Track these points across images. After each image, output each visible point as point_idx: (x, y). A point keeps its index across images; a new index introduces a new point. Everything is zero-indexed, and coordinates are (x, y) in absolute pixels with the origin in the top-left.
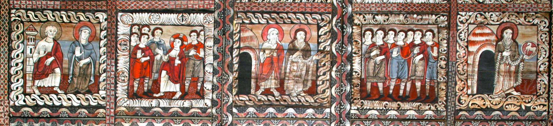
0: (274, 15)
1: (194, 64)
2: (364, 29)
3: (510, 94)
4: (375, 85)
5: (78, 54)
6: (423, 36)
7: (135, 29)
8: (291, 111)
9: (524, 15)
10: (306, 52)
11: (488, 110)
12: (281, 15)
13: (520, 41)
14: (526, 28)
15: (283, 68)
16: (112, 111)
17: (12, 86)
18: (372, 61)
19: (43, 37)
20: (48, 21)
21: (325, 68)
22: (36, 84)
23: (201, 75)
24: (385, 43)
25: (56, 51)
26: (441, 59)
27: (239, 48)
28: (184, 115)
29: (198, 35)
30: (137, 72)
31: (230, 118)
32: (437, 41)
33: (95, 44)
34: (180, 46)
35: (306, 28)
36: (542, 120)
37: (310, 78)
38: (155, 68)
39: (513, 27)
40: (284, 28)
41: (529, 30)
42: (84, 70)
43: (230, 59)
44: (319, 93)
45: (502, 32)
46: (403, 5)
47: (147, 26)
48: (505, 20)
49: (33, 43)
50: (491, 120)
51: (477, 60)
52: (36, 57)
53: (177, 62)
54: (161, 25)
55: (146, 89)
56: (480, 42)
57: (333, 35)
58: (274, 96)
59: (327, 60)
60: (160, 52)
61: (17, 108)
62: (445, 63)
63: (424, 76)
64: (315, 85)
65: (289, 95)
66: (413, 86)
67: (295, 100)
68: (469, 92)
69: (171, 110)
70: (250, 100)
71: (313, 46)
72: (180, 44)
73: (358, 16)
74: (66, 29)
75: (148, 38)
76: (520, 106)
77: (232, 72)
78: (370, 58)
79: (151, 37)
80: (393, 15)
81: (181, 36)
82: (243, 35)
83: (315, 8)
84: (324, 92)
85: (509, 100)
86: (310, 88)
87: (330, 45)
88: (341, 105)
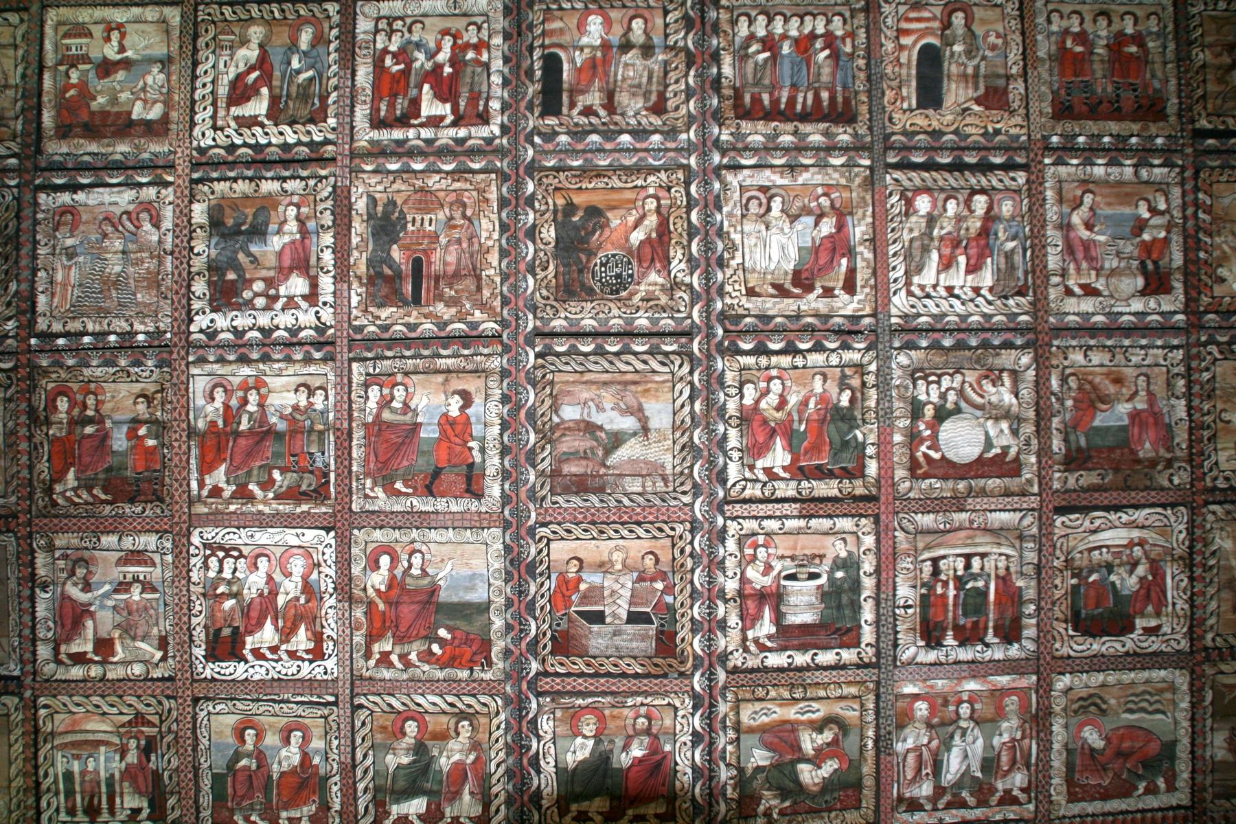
1: (473, 72)
2: (735, 14)
3: (968, 109)
5: (295, 64)
6: (829, 22)
7: (383, 25)
10: (647, 50)
11: (936, 134)
13: (979, 30)
16: (347, 147)
17: (197, 117)
18: (751, 61)
19: (244, 42)
20: (252, 18)
23: (484, 88)
24: (770, 34)
25: (263, 63)
27: (543, 46)
28: (459, 149)
29: (479, 28)
30: (385, 88)
33: (321, 49)
35: (646, 14)
36: (1020, 148)
37: (654, 88)
41: (990, 13)
42: (304, 88)
43: (529, 62)
47: (402, 19)
49: (228, 52)
50: (941, 149)
53: (448, 70)
55: (398, 112)
57: (688, 22)
58: (598, 116)
59: (679, 61)
60: (421, 56)
61: (202, 151)
62: (864, 61)
63: (833, 83)
64: (662, 98)
65: (623, 114)
66: (817, 97)
67: (633, 122)
68: (905, 106)
70: (561, 124)
71: (657, 39)
72: (451, 43)
74: (279, 29)
76: (985, 127)
77: (532, 82)
78: (747, 56)
79: (407, 35)
81: (453, 31)
84: (677, 108)
86: (655, 104)
87: (685, 38)
88: (704, 127)
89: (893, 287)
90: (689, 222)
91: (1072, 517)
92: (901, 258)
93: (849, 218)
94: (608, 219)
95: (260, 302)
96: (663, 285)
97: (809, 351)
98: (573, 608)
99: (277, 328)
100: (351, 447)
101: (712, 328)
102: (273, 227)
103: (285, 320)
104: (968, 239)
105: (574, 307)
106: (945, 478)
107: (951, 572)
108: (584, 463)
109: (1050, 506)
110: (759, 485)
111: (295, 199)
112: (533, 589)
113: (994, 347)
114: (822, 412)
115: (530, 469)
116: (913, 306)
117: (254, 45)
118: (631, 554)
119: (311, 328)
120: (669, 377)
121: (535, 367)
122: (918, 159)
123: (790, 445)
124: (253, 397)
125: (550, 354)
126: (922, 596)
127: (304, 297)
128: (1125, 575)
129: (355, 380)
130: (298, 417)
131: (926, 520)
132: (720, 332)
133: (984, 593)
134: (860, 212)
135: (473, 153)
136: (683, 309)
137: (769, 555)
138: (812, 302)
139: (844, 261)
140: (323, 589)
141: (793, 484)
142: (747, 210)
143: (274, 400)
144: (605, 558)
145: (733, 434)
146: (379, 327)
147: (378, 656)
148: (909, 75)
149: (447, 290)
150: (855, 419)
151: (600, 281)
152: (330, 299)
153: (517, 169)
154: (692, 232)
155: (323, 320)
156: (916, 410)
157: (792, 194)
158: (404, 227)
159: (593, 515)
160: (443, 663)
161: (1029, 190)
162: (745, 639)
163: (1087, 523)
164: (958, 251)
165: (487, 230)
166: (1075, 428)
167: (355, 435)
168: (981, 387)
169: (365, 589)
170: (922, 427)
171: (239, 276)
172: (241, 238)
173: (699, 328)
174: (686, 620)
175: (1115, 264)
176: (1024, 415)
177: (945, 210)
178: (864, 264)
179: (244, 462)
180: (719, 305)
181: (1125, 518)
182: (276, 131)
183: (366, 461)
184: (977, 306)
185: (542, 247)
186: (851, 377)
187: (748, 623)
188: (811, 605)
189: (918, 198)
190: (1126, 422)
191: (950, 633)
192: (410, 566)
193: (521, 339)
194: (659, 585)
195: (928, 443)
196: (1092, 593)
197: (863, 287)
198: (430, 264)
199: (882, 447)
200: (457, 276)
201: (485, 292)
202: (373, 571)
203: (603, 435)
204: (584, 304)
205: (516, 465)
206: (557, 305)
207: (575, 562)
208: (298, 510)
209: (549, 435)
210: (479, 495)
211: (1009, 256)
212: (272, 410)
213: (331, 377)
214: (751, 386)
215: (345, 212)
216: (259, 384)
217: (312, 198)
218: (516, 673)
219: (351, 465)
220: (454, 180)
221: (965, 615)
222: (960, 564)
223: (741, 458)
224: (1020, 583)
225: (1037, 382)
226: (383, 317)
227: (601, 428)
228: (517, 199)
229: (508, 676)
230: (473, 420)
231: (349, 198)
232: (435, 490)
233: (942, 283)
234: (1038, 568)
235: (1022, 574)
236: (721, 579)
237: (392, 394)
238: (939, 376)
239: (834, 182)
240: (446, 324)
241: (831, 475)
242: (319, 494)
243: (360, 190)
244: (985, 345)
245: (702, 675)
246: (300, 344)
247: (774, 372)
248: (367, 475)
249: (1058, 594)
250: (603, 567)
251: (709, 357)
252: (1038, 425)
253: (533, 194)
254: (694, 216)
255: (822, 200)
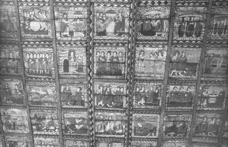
6: (45, 55)
13: (77, 56)
39: (74, 51)
45: (70, 53)
51: (63, 62)
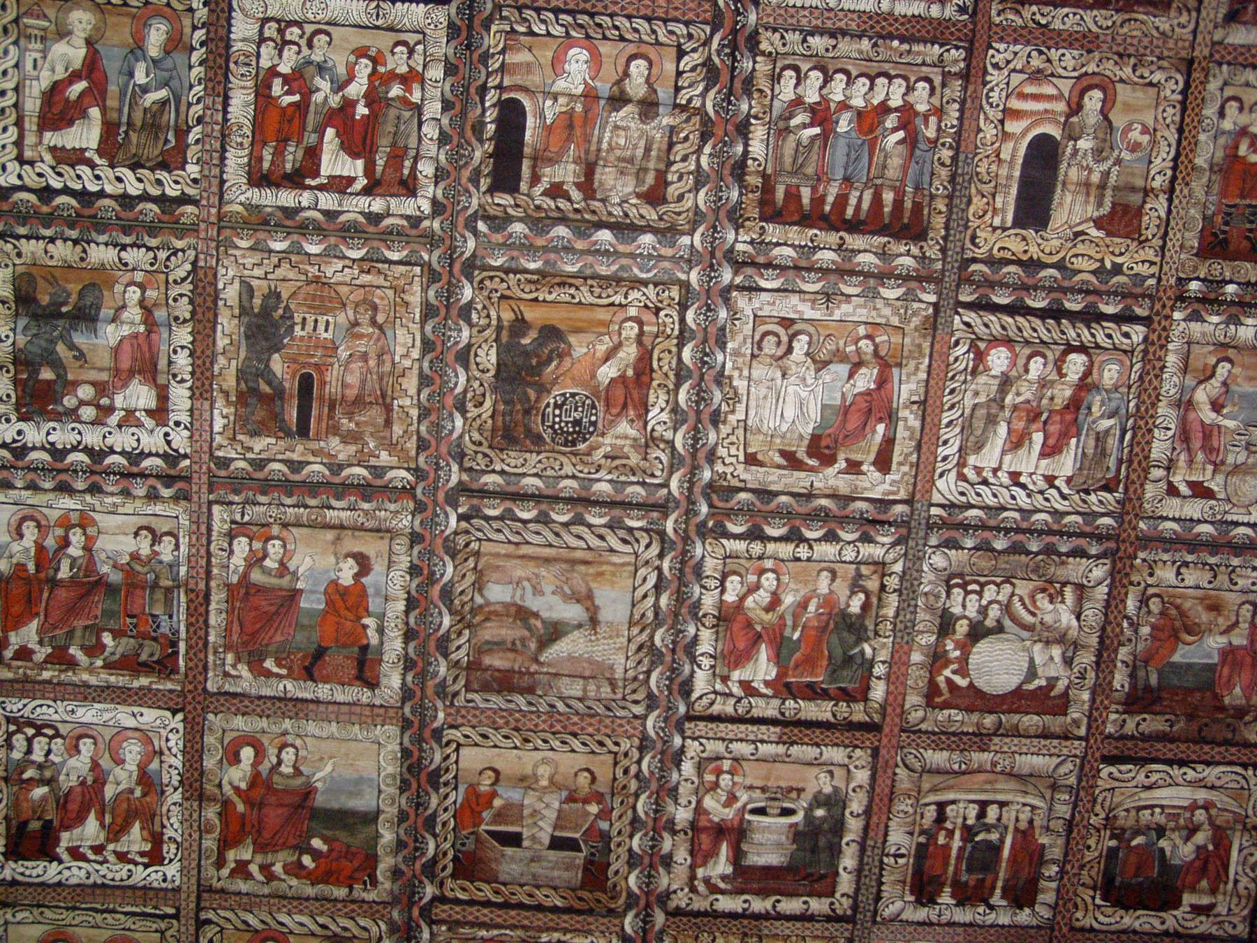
0: (583, 19)
2: (779, 65)
3: (1083, 233)
4: (793, 190)
5: (140, 77)
6: (910, 89)
7: (271, 30)
8: (605, 235)
9: (1132, 61)
10: (648, 107)
11: (1032, 265)
12: (597, 20)
13: (1118, 119)
14: (1134, 91)
15: (595, 139)
16: (214, 211)
18: (792, 137)
19: (63, 33)
21: (686, 145)
22: (45, 141)
23: (413, 142)
24: (825, 100)
25: (92, 68)
26: (943, 145)
27: (500, 87)
28: (371, 229)
29: (411, 52)
31: (471, 244)
32: (937, 104)
33: (179, 58)
34: (370, 76)
36: (1143, 296)
38: (311, 118)
39: (1107, 86)
40: (602, 50)
41: (1140, 94)
42: (154, 116)
43: (479, 111)
44: (670, 199)
46: (870, 18)
48: (1091, 68)
49: (39, 46)
50: (1035, 288)
51: (1022, 152)
52: (45, 82)
53: (362, 110)
54: (328, 23)
55: (289, 166)
56: (1033, 113)
57: (711, 74)
58: (569, 200)
59: (691, 129)
60: (324, 85)
62: (951, 153)
64: (662, 181)
65: (603, 201)
66: (877, 200)
67: (617, 211)
68: (997, 221)
69: (343, 218)
70: (517, 206)
71: (664, 94)
72: (369, 70)
73: (769, 34)
75: (299, 53)
76: (1102, 261)
77: (481, 141)
78: (787, 130)
80: (847, 39)
81: (372, 52)
82: (511, 58)
83: (676, 9)
84: (681, 198)
85: (1080, 246)
86: (652, 189)
87: (703, 95)
88: (715, 231)
89: (940, 467)
90: (680, 359)
91: (1124, 768)
92: (958, 430)
93: (895, 371)
94: (570, 346)
95: (88, 413)
96: (635, 440)
97: (818, 540)
98: (483, 827)
99: (112, 451)
100: (207, 612)
101: (694, 503)
102: (106, 312)
103: (123, 440)
104: (1051, 412)
105: (512, 460)
106: (970, 710)
107: (960, 821)
108: (511, 655)
109: (1098, 755)
110: (732, 701)
111: (139, 276)
112: (434, 801)
113: (1060, 554)
114: (824, 618)
115: (441, 659)
116: (962, 494)
117: (79, 39)
118: (562, 769)
119: (157, 455)
120: (632, 559)
121: (456, 533)
122: (1002, 299)
123: (778, 656)
124: (76, 537)
125: (477, 517)
126: (919, 845)
127: (149, 412)
128: (1178, 841)
129: (215, 528)
130: (138, 568)
131: (937, 758)
132: (704, 509)
133: (996, 849)
134: (912, 364)
135: (390, 236)
136: (658, 473)
137: (734, 784)
138: (831, 478)
139: (881, 428)
140: (165, 781)
141: (776, 702)
142: (760, 348)
143: (105, 545)
144: (528, 770)
145: (706, 635)
146: (251, 462)
147: (233, 865)
148: (1009, 177)
149: (344, 421)
150: (866, 630)
151: (552, 427)
152: (185, 418)
153: (451, 265)
154: (681, 374)
155: (174, 446)
156: (946, 624)
157: (824, 332)
158: (291, 328)
159: (517, 721)
160: (314, 878)
161: (1145, 352)
162: (693, 877)
163: (1141, 777)
164: (1034, 427)
165: (404, 345)
166: (1146, 662)
167: (214, 598)
168: (1034, 602)
169: (220, 786)
170: (950, 646)
171: (58, 376)
172: (61, 322)
173: (677, 503)
174: (622, 851)
175: (1241, 458)
176: (1084, 640)
177: (1027, 371)
178: (907, 434)
179: (63, 621)
180: (707, 475)
181: (1191, 774)
182: (112, 176)
183: (228, 629)
184: (1047, 500)
185: (477, 373)
186: (868, 577)
187: (699, 861)
188: (779, 845)
189: (993, 352)
190: (1216, 660)
191: (948, 889)
192: (280, 762)
193: (441, 496)
194: (593, 809)
195: (954, 666)
196: (1133, 859)
197: (900, 464)
198: (323, 383)
199: (895, 668)
200: (359, 402)
201: (395, 428)
202: (231, 764)
203: (539, 624)
204: (528, 455)
205: (423, 653)
206: (492, 454)
207: (490, 773)
208: (136, 684)
209: (465, 621)
210: (373, 685)
211: (1100, 438)
212: (103, 556)
213: (184, 521)
214: (736, 578)
215: (209, 304)
216: (84, 522)
217: (163, 276)
218: (407, 896)
219: (207, 634)
220: (362, 271)
221: (969, 870)
222: (973, 811)
223: (712, 667)
224: (1044, 840)
225: (1107, 601)
226: (257, 449)
227: (536, 615)
228: (447, 307)
229: (394, 901)
230: (370, 591)
231: (214, 284)
232: (316, 674)
233: (1005, 467)
234: (1070, 825)
235: (1048, 829)
236: (671, 808)
237: (265, 549)
238: (982, 585)
239: (883, 321)
240: (341, 467)
241: (825, 695)
242: (165, 667)
243: (231, 273)
244: (1049, 550)
245: (637, 916)
246: (142, 475)
247: (769, 564)
248: (228, 648)
249: (1089, 856)
250: (525, 781)
251: (686, 539)
252: (1099, 655)
253: (471, 302)
254: (687, 354)
255: (862, 343)
